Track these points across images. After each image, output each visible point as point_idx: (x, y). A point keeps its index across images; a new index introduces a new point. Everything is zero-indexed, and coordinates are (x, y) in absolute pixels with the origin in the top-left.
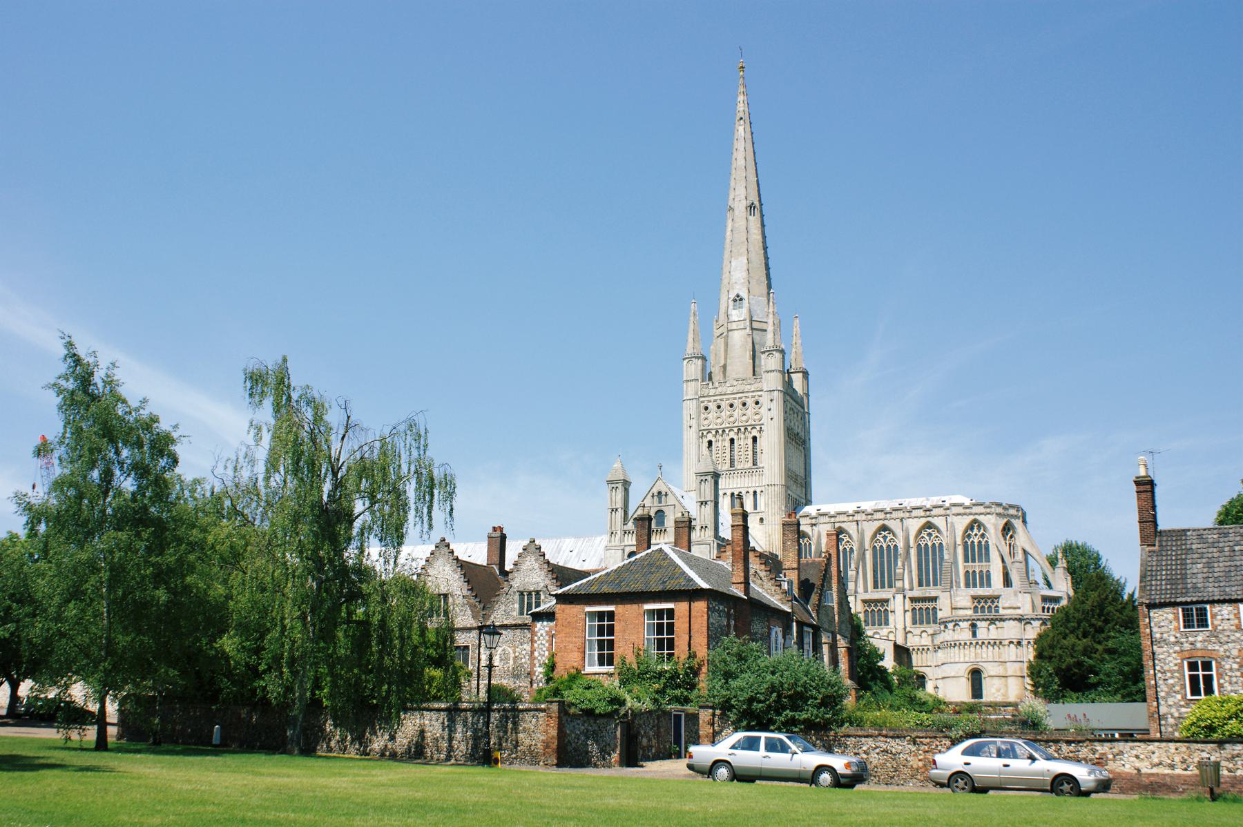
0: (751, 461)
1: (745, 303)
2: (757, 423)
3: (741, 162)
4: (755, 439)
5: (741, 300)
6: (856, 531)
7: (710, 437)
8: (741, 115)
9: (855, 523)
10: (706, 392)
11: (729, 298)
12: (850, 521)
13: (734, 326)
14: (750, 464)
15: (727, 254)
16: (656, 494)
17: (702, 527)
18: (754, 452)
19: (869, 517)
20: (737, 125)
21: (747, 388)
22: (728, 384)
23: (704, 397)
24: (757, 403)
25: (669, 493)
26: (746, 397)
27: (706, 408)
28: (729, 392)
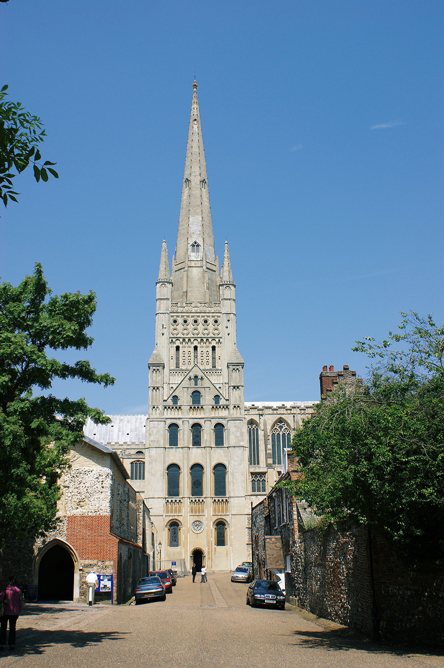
0: (211, 364)
1: (201, 248)
2: (216, 336)
3: (195, 149)
4: (214, 348)
5: (198, 246)
6: (293, 421)
7: (178, 344)
8: (195, 117)
9: (292, 415)
10: (175, 309)
11: (188, 244)
12: (289, 414)
13: (199, 264)
14: (210, 367)
15: (183, 212)
16: (192, 377)
17: (235, 407)
18: (214, 358)
19: (303, 411)
20: (191, 124)
21: (208, 310)
22: (193, 305)
23: (173, 313)
24: (216, 321)
25: (204, 377)
26: (208, 316)
27: (175, 321)
28: (193, 311)
